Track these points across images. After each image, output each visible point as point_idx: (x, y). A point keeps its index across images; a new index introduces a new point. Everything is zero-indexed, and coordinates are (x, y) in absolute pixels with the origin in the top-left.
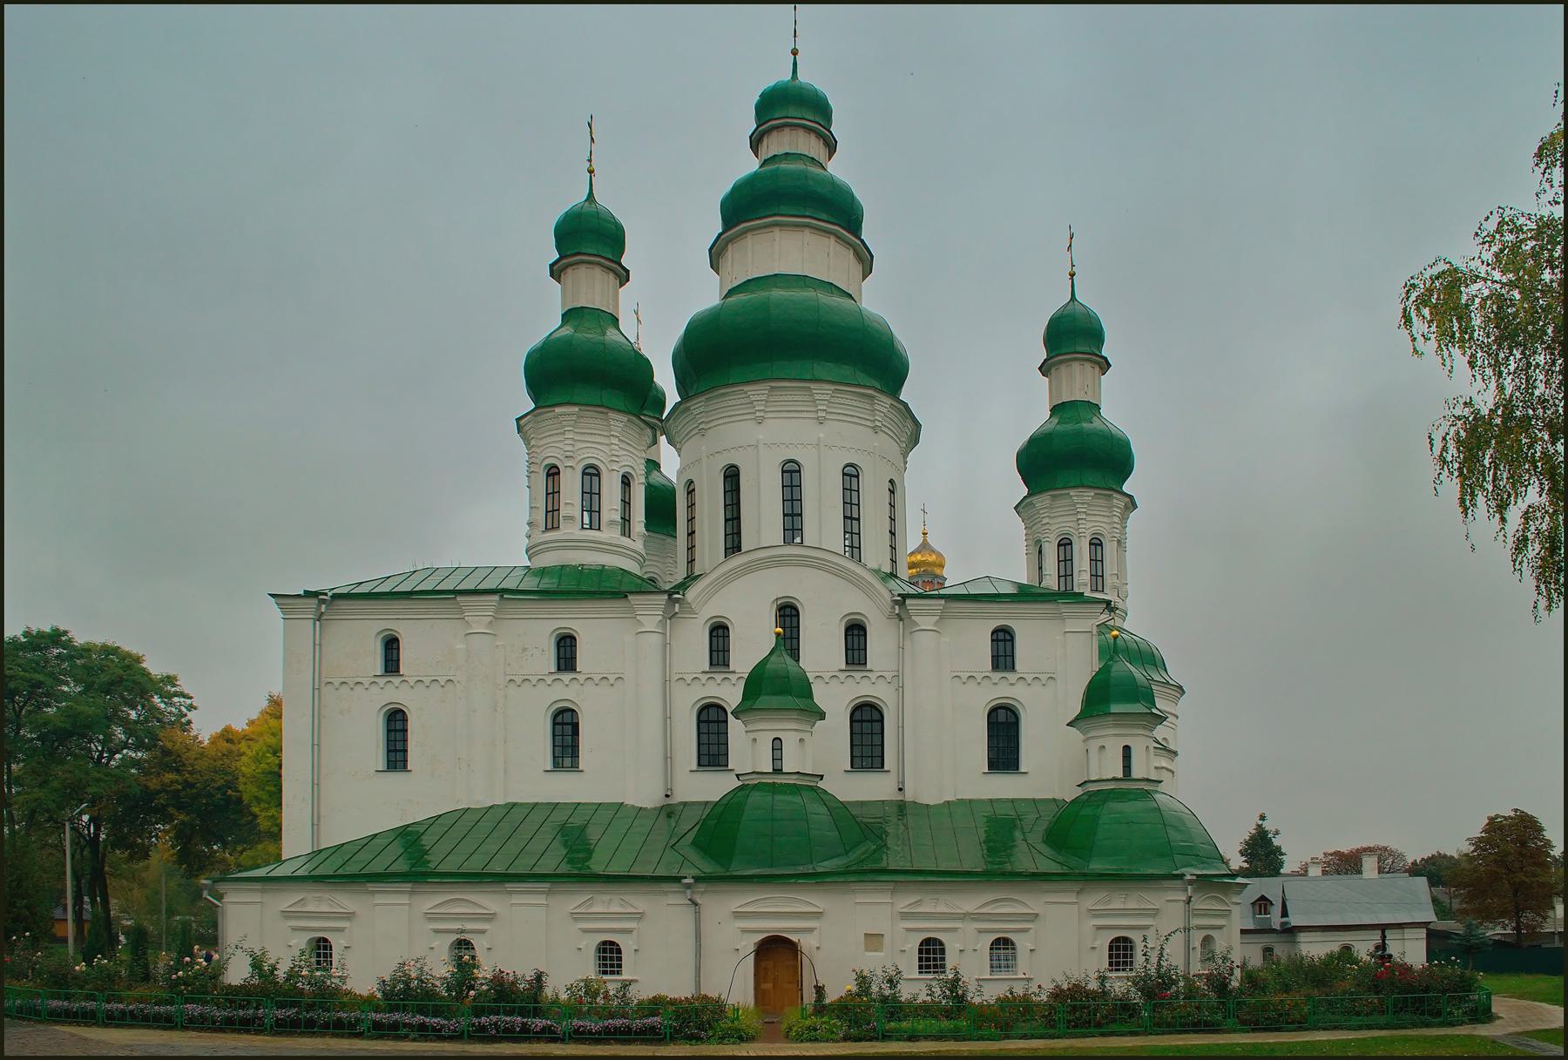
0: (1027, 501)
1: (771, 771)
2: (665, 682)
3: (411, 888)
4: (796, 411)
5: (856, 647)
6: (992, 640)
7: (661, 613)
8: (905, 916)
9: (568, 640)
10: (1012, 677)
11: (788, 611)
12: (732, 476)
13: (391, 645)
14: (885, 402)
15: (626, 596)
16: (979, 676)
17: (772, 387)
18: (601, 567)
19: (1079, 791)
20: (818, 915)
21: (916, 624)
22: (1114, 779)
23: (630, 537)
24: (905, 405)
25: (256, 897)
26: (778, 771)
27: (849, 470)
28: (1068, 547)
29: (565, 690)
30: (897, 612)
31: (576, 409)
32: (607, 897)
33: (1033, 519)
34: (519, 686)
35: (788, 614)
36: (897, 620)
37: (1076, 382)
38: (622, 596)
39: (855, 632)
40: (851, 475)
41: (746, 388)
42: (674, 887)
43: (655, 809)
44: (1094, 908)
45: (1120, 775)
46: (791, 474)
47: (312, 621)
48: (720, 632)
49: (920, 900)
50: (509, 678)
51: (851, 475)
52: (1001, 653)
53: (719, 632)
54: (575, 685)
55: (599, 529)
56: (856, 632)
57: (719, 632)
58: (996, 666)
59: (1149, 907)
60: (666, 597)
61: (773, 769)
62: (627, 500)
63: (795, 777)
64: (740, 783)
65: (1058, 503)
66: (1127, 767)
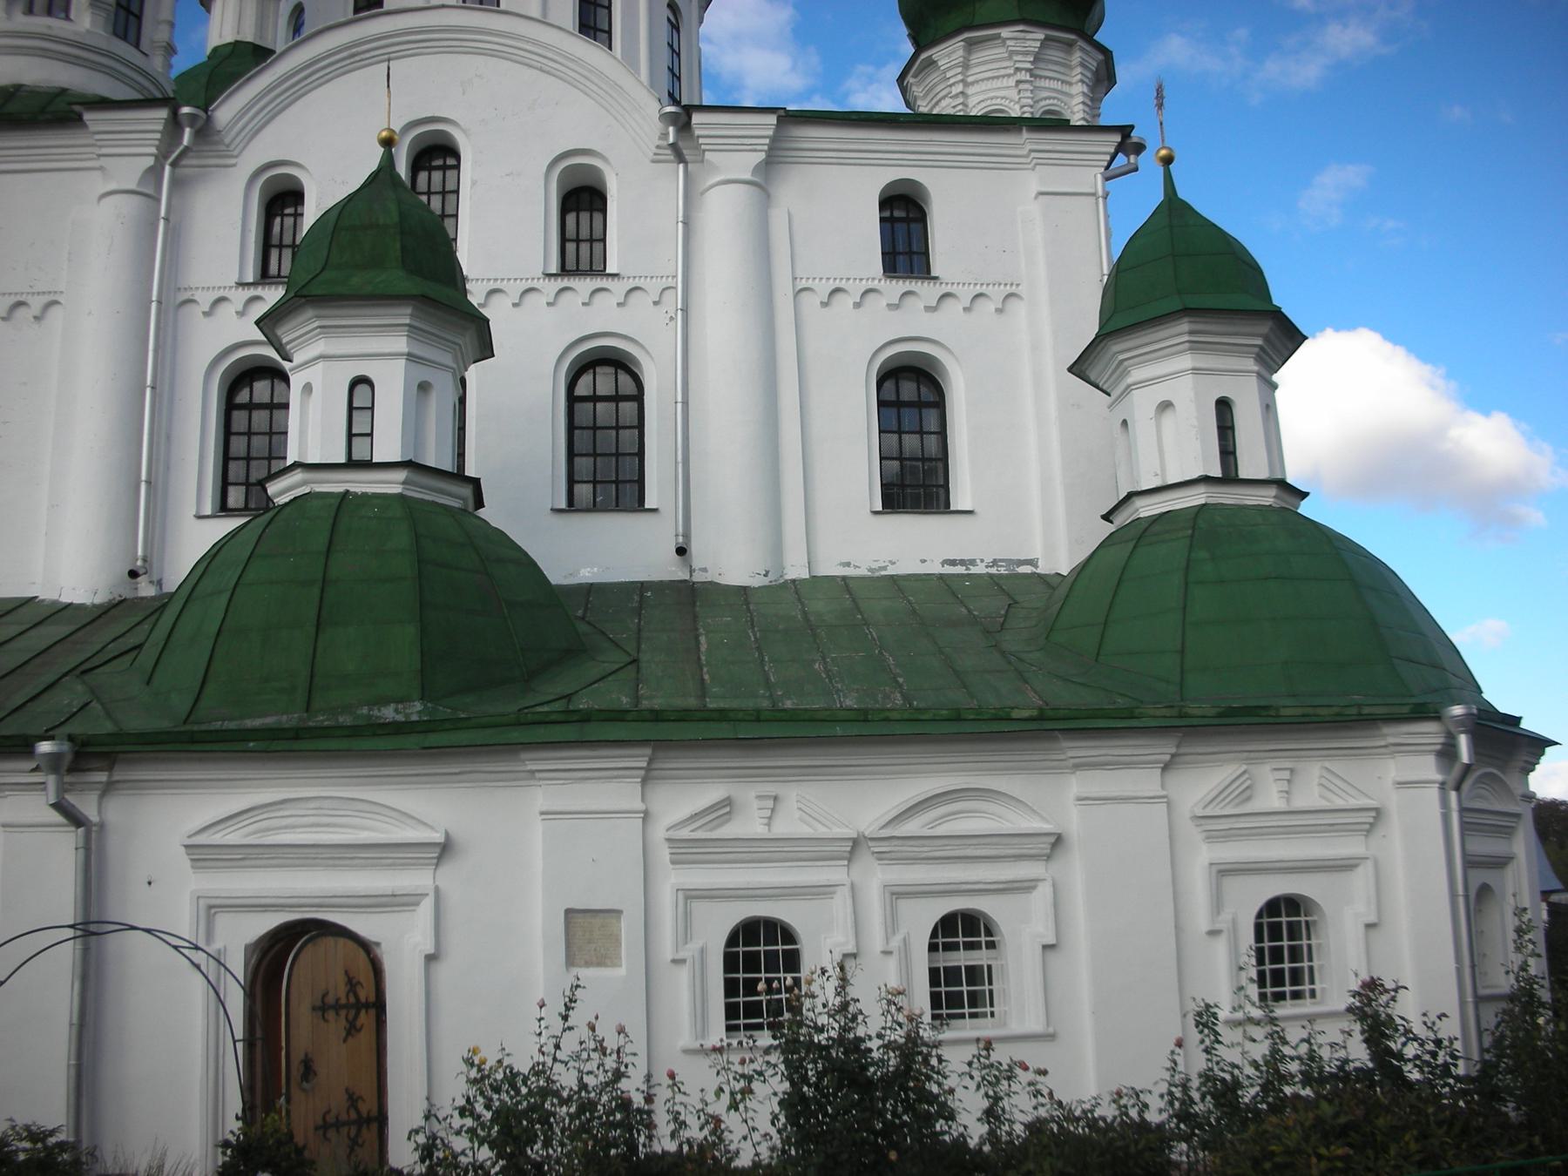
0: (923, 56)
5: (584, 233)
7: (153, 150)
8: (686, 851)
19: (1109, 528)
22: (1206, 480)
30: (671, 140)
33: (931, 95)
44: (1208, 812)
45: (1217, 472)
49: (728, 802)
52: (900, 248)
59: (1353, 803)
63: (401, 475)
65: (979, 56)
66: (1228, 452)
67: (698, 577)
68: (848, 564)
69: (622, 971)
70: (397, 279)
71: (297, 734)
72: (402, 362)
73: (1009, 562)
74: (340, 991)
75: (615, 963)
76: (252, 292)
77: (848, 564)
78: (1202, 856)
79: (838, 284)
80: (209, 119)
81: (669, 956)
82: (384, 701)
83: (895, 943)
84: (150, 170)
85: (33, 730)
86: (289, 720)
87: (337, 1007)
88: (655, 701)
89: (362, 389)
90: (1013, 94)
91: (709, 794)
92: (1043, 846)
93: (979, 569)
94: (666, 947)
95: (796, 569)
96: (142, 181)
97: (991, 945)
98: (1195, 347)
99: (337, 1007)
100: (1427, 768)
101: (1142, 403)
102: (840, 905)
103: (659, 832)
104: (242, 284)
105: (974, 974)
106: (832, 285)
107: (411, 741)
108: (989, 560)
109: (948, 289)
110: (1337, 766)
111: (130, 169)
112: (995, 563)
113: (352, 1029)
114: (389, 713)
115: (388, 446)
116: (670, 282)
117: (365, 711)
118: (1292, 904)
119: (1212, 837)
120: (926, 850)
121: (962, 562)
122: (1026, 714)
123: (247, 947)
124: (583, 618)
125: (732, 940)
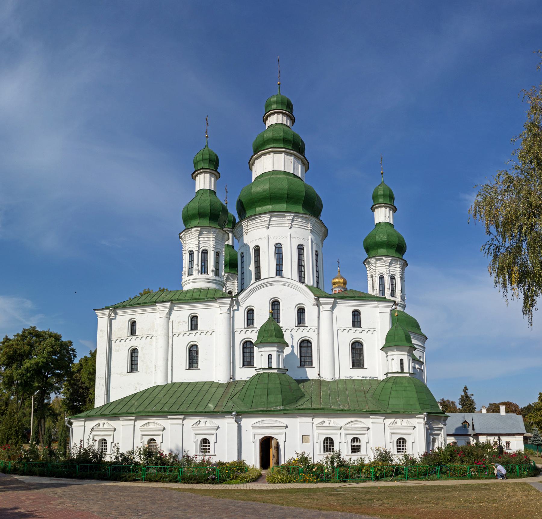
1: (268, 367)
4: (280, 224)
6: (352, 315)
7: (229, 305)
8: (318, 428)
9: (195, 318)
10: (360, 330)
11: (276, 303)
12: (257, 250)
14: (314, 219)
15: (216, 299)
16: (348, 329)
18: (208, 289)
23: (219, 276)
24: (321, 221)
26: (270, 368)
27: (300, 247)
28: (383, 279)
29: (193, 337)
32: (205, 420)
35: (275, 304)
36: (316, 306)
38: (214, 299)
39: (301, 311)
40: (300, 248)
41: (262, 216)
43: (226, 384)
44: (390, 425)
46: (279, 248)
48: (251, 311)
51: (300, 248)
53: (250, 312)
55: (207, 274)
56: (301, 311)
57: (250, 312)
58: (354, 326)
60: (230, 299)
61: (269, 367)
62: (218, 262)
64: (257, 373)
67: (321, 379)
68: (346, 377)
69: (310, 444)
70: (275, 339)
71: (266, 411)
72: (276, 352)
73: (373, 377)
75: (309, 443)
76: (247, 329)
77: (346, 377)
78: (388, 431)
79: (345, 328)
80: (238, 299)
81: (316, 442)
82: (277, 406)
83: (346, 441)
84: (228, 309)
85: (232, 410)
86: (265, 409)
88: (314, 406)
89: (270, 356)
91: (322, 420)
92: (367, 429)
93: (368, 378)
94: (315, 441)
95: (337, 378)
96: (227, 311)
97: (360, 442)
101: (390, 358)
102: (339, 435)
103: (314, 425)
104: (245, 328)
105: (358, 446)
106: (344, 328)
107: (281, 412)
108: (369, 377)
109: (364, 329)
110: (409, 420)
111: (225, 309)
112: (370, 377)
114: (278, 408)
115: (274, 365)
116: (316, 328)
117: (275, 407)
118: (403, 439)
119: (390, 429)
120: (350, 428)
121: (365, 377)
122: (364, 411)
123: (260, 440)
124: (303, 388)
125: (324, 440)
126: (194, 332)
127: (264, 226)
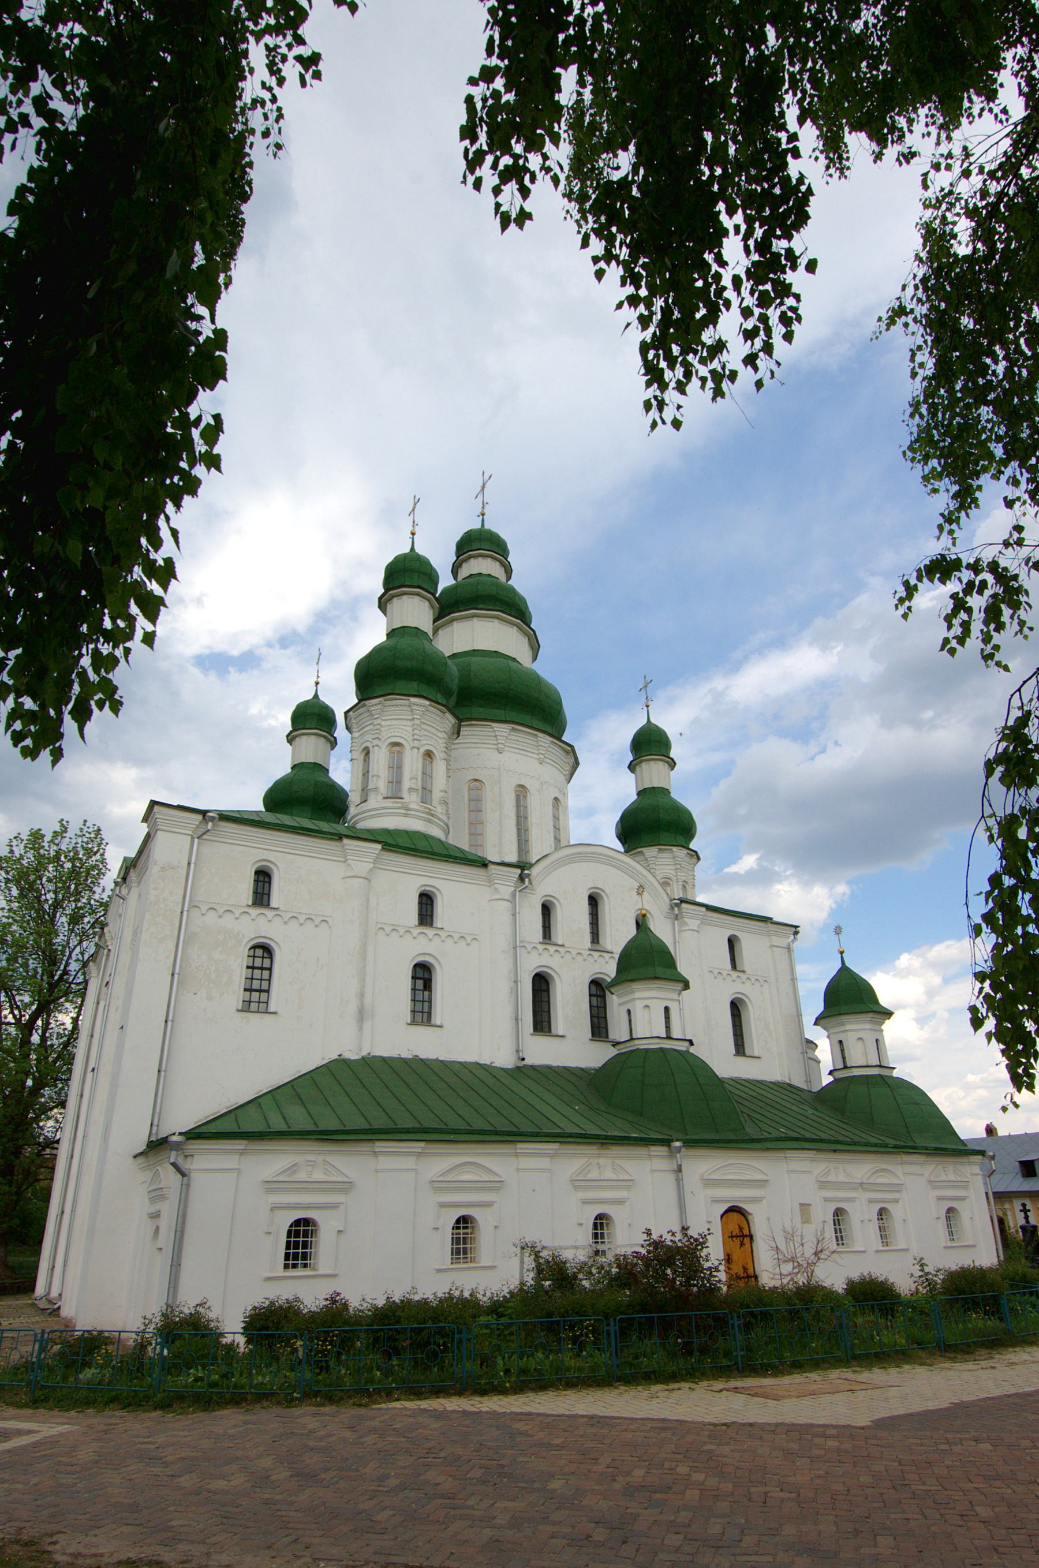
2: (515, 948)
3: (423, 1148)
8: (823, 1185)
13: (263, 877)
16: (725, 973)
17: (513, 729)
20: (762, 1183)
21: (686, 924)
25: (231, 1161)
31: (427, 703)
34: (414, 938)
37: (654, 773)
41: (494, 725)
42: (661, 1150)
47: (190, 837)
50: (380, 926)
54: (436, 939)
74: (737, 1232)
87: (737, 1236)
90: (673, 873)
98: (871, 1022)
99: (737, 1236)
100: (976, 1169)
104: (540, 943)
113: (742, 1244)
126: (430, 932)
127: (495, 747)
